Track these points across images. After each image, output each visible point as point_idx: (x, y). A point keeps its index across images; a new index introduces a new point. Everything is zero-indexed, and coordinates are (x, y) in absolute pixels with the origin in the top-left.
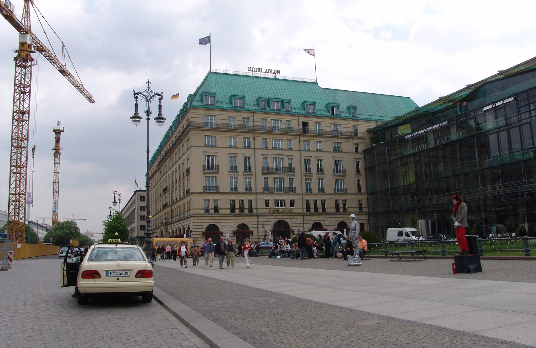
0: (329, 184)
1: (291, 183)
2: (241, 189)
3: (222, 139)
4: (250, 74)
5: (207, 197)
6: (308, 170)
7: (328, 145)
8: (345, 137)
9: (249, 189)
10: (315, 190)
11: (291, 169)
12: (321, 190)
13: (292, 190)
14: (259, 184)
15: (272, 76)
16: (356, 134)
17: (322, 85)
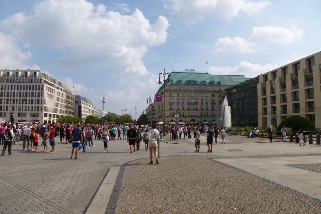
0: (210, 107)
1: (196, 107)
2: (180, 109)
3: (175, 94)
4: (185, 71)
5: (170, 111)
6: (202, 103)
7: (209, 95)
8: (215, 91)
9: (183, 109)
10: (204, 109)
11: (196, 103)
12: (207, 109)
13: (197, 109)
14: (186, 107)
15: (192, 71)
16: (220, 91)
17: (210, 73)
